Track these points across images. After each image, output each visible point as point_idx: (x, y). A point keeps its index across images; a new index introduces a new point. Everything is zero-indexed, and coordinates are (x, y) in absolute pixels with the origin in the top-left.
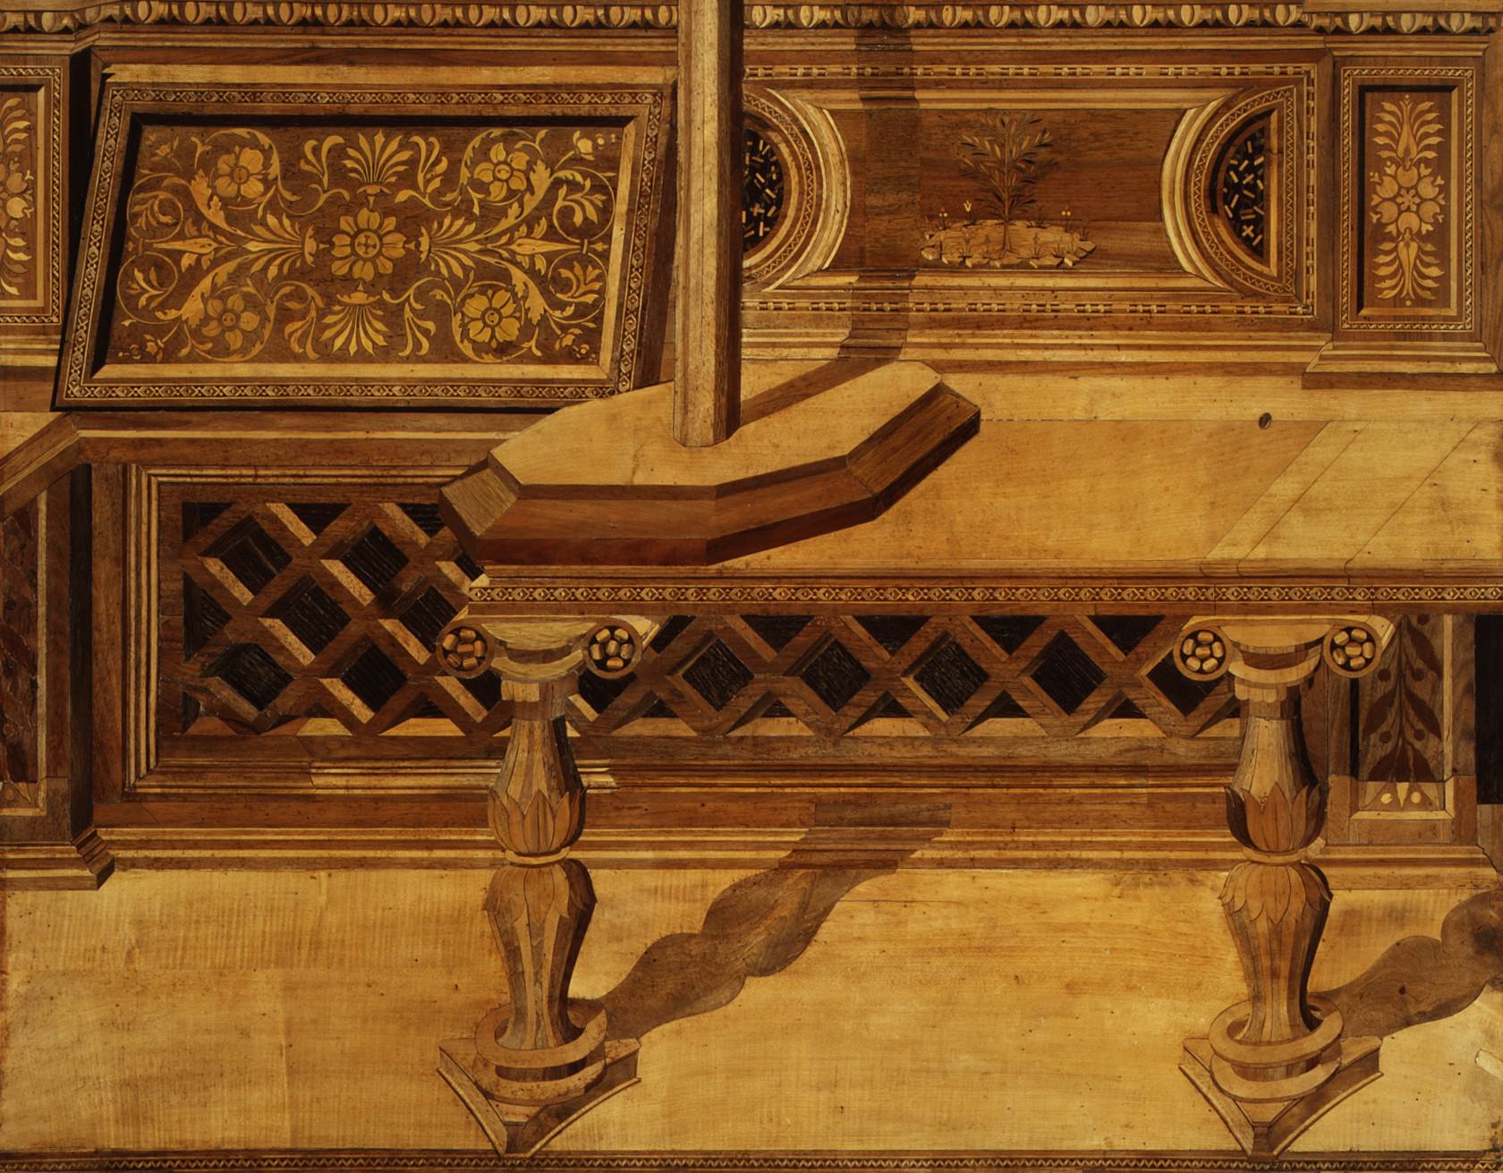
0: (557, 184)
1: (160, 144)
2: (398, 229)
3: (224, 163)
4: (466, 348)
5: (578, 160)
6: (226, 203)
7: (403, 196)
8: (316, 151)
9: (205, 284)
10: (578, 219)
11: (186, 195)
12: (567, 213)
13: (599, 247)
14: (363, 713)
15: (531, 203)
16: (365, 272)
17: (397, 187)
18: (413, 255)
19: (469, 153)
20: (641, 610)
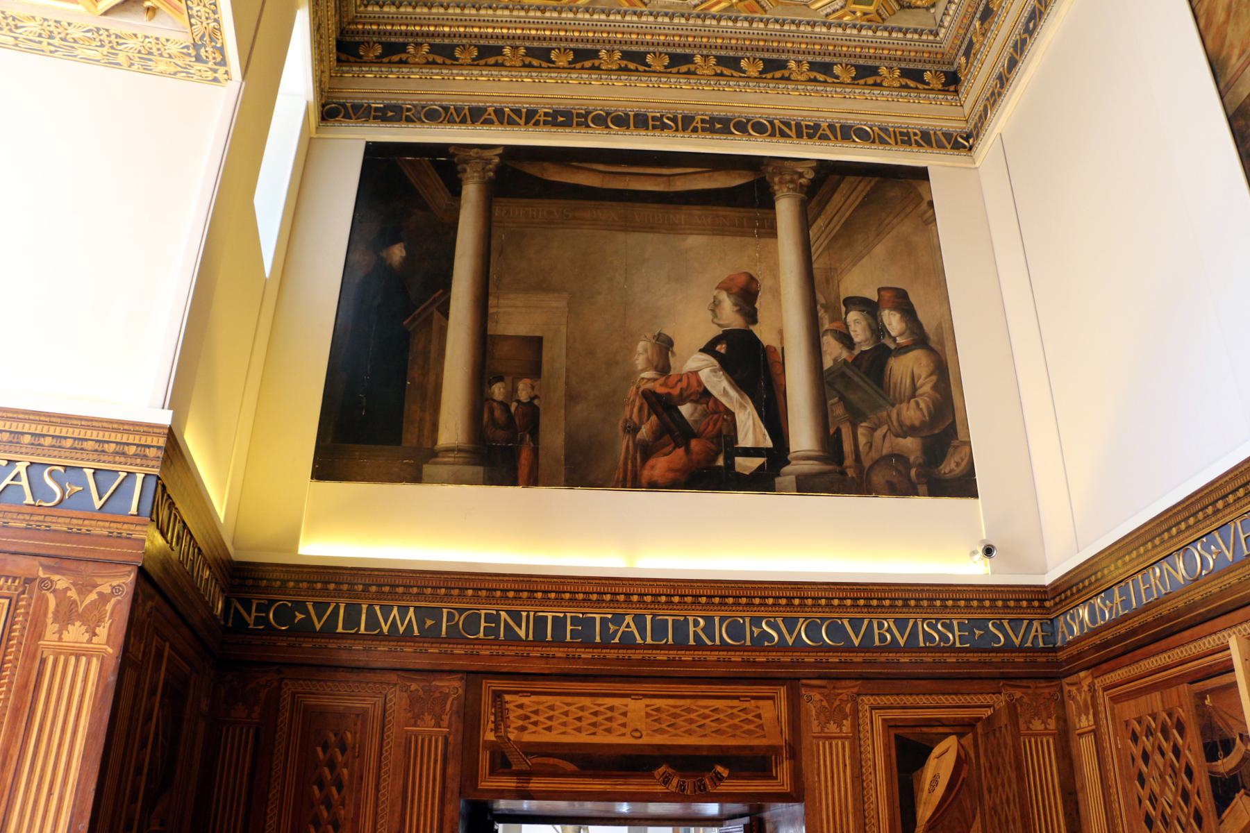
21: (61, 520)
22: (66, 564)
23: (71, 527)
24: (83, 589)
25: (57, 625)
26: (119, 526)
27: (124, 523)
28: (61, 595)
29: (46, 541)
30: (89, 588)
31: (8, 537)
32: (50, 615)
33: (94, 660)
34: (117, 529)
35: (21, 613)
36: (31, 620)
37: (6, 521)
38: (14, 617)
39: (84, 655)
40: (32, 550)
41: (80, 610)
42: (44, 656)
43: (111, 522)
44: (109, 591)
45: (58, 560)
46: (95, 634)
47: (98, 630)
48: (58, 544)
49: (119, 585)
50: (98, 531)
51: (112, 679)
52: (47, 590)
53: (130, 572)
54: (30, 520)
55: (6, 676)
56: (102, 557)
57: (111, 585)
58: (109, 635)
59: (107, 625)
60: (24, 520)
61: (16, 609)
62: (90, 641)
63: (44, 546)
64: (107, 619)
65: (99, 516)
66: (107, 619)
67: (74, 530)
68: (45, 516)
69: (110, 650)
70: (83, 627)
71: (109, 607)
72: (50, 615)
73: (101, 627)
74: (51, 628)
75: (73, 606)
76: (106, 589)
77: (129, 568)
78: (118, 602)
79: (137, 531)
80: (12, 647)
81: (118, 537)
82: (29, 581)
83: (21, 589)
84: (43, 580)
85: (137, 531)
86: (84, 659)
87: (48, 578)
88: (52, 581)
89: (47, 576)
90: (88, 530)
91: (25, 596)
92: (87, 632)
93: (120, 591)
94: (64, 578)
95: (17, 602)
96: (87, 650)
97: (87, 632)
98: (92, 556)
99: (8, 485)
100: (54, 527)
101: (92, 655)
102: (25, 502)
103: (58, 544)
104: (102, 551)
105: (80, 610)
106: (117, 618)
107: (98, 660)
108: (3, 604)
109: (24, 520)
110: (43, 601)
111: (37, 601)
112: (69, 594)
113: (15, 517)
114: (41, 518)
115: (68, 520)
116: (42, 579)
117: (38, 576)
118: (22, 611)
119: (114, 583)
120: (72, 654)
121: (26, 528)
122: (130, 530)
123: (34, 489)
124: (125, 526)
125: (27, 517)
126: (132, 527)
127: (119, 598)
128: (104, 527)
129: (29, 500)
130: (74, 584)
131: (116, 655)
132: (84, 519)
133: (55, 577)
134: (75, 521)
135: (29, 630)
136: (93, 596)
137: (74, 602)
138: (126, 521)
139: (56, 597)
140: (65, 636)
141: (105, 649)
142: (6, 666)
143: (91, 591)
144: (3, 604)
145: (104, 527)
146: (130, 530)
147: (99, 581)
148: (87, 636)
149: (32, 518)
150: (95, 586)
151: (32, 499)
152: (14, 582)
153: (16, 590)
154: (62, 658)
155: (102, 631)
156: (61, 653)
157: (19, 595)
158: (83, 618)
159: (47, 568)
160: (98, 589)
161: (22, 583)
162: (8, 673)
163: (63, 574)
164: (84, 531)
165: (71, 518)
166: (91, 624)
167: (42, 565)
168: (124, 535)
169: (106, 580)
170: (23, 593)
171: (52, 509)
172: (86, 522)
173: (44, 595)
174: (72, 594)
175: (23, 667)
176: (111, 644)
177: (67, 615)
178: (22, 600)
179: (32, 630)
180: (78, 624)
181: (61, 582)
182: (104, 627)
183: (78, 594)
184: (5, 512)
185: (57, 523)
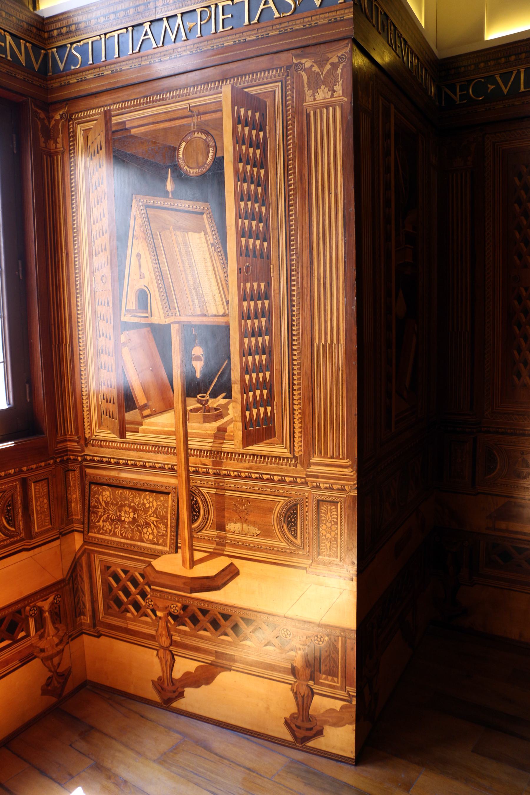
0: (157, 505)
1: (94, 488)
2: (132, 512)
3: (104, 493)
4: (145, 540)
5: (161, 501)
6: (105, 502)
7: (132, 504)
8: (118, 493)
9: (102, 519)
10: (161, 514)
11: (98, 498)
12: (160, 512)
13: (166, 521)
14: (136, 613)
15: (153, 509)
16: (127, 520)
17: (131, 502)
18: (134, 518)
19: (142, 497)
20: (179, 602)
21: (298, 22)
22: (308, 50)
23: (305, 24)
24: (321, 64)
25: (311, 91)
26: (334, 14)
27: (337, 11)
28: (309, 71)
29: (291, 38)
30: (325, 62)
31: (270, 43)
32: (306, 86)
33: (337, 107)
34: (333, 16)
35: (289, 89)
36: (296, 92)
37: (267, 33)
38: (286, 93)
39: (331, 106)
40: (286, 47)
41: (322, 77)
42: (308, 112)
43: (328, 13)
44: (337, 61)
45: (302, 49)
46: (334, 91)
47: (335, 88)
48: (300, 38)
49: (342, 55)
50: (322, 22)
51: (350, 117)
52: (301, 70)
53: (348, 44)
54: (280, 28)
55: (290, 128)
56: (328, 39)
57: (337, 56)
58: (343, 89)
59: (340, 83)
60: (277, 29)
61: (286, 87)
62: (332, 96)
63: (292, 42)
64: (339, 79)
65: (321, 11)
66: (339, 79)
67: (307, 26)
68: (288, 22)
69: (345, 99)
70: (326, 88)
71: (339, 71)
72: (306, 86)
73: (337, 86)
74: (308, 93)
75: (318, 76)
76: (335, 60)
77: (346, 42)
78: (344, 67)
79: (346, 13)
80: (290, 111)
81: (335, 22)
82: (288, 67)
83: (285, 74)
84: (296, 65)
85: (346, 13)
86: (331, 109)
87: (300, 63)
88: (302, 64)
89: (298, 61)
90: (315, 23)
91: (289, 77)
92: (329, 91)
93: (343, 58)
94: (308, 60)
95: (286, 82)
96: (331, 102)
97: (329, 91)
98: (322, 40)
99: (262, 10)
100: (295, 28)
101: (335, 105)
102: (274, 17)
103: (300, 38)
104: (328, 35)
105: (322, 77)
106: (346, 77)
107: (339, 107)
108: (278, 86)
109: (277, 29)
110: (300, 77)
111: (296, 78)
112: (314, 69)
113: (271, 29)
114: (286, 24)
115: (302, 20)
116: (296, 64)
117: (294, 63)
118: (290, 87)
119: (339, 55)
120: (323, 107)
121: (280, 34)
122: (342, 14)
123: (278, 7)
124: (338, 13)
125: (278, 26)
126: (343, 12)
127: (344, 63)
128: (325, 18)
129: (277, 15)
130: (315, 62)
131: (350, 101)
132: (312, 16)
133: (303, 61)
134: (306, 20)
135: (296, 98)
136: (328, 67)
137: (318, 73)
138: (338, 8)
139: (306, 73)
140: (317, 96)
141: (343, 99)
142: (289, 123)
143: (326, 64)
144: (278, 86)
145: (325, 18)
146: (342, 14)
147: (329, 55)
148: (330, 93)
149: (281, 26)
150: (328, 60)
151: (278, 14)
152: (281, 70)
153: (283, 75)
154: (318, 110)
155: (338, 88)
156: (317, 108)
157: (285, 78)
158: (325, 83)
159: (297, 56)
160: (330, 61)
161: (285, 69)
162: (291, 127)
163: (307, 58)
164: (313, 24)
165: (304, 18)
166: (331, 85)
167: (293, 55)
168: (339, 19)
169: (334, 53)
170: (287, 76)
171: (291, 16)
172: (313, 18)
173: (300, 73)
174: (316, 69)
175: (298, 122)
176: (345, 95)
177: (315, 84)
178: (288, 80)
179: (298, 97)
180: (323, 87)
181: (307, 63)
182: (339, 85)
183: (319, 68)
184: (265, 27)
185: (296, 24)
